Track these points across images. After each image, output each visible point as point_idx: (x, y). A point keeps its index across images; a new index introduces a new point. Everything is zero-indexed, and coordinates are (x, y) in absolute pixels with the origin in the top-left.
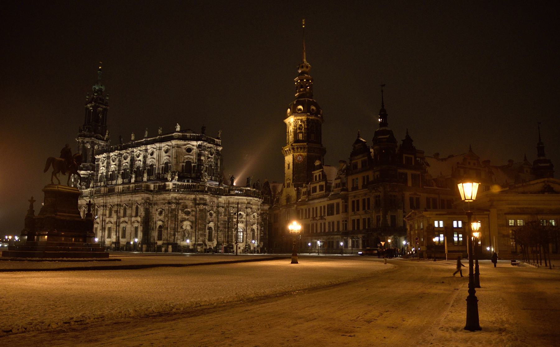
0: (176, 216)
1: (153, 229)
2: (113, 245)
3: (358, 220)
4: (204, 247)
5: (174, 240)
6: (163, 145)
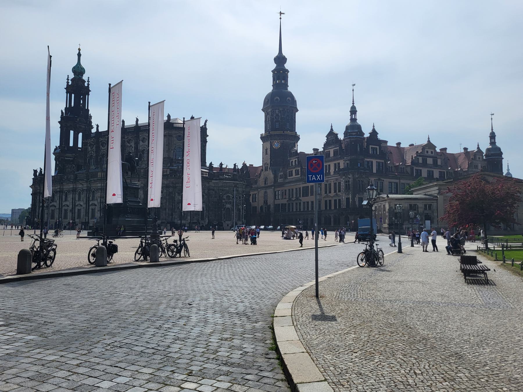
3: (330, 201)
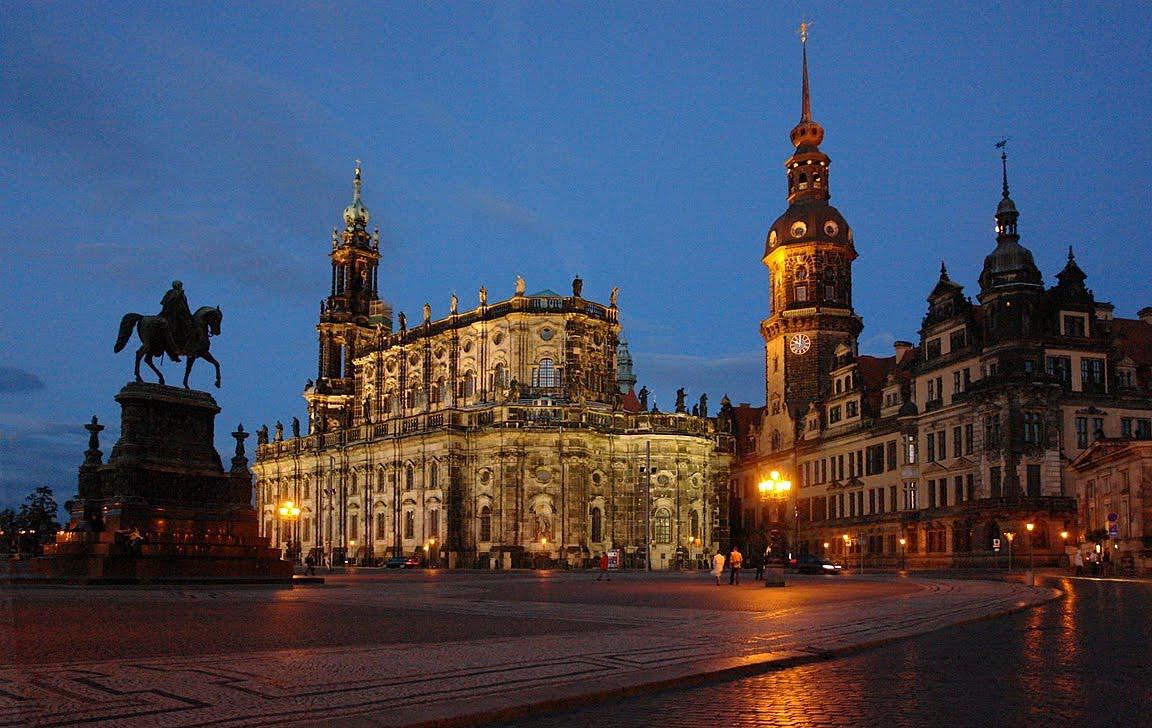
0: (518, 484)
1: (470, 516)
2: (390, 555)
3: (943, 482)
4: (583, 556)
5: (516, 538)
6: (490, 325)
